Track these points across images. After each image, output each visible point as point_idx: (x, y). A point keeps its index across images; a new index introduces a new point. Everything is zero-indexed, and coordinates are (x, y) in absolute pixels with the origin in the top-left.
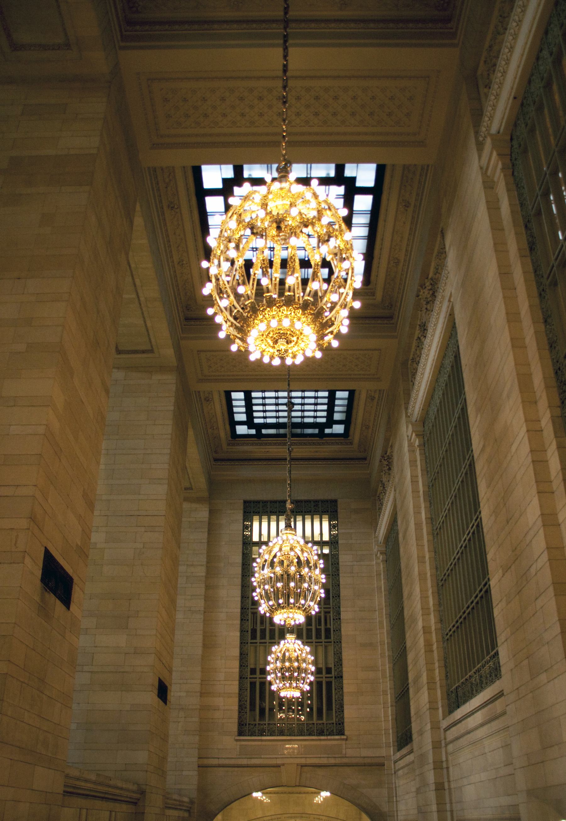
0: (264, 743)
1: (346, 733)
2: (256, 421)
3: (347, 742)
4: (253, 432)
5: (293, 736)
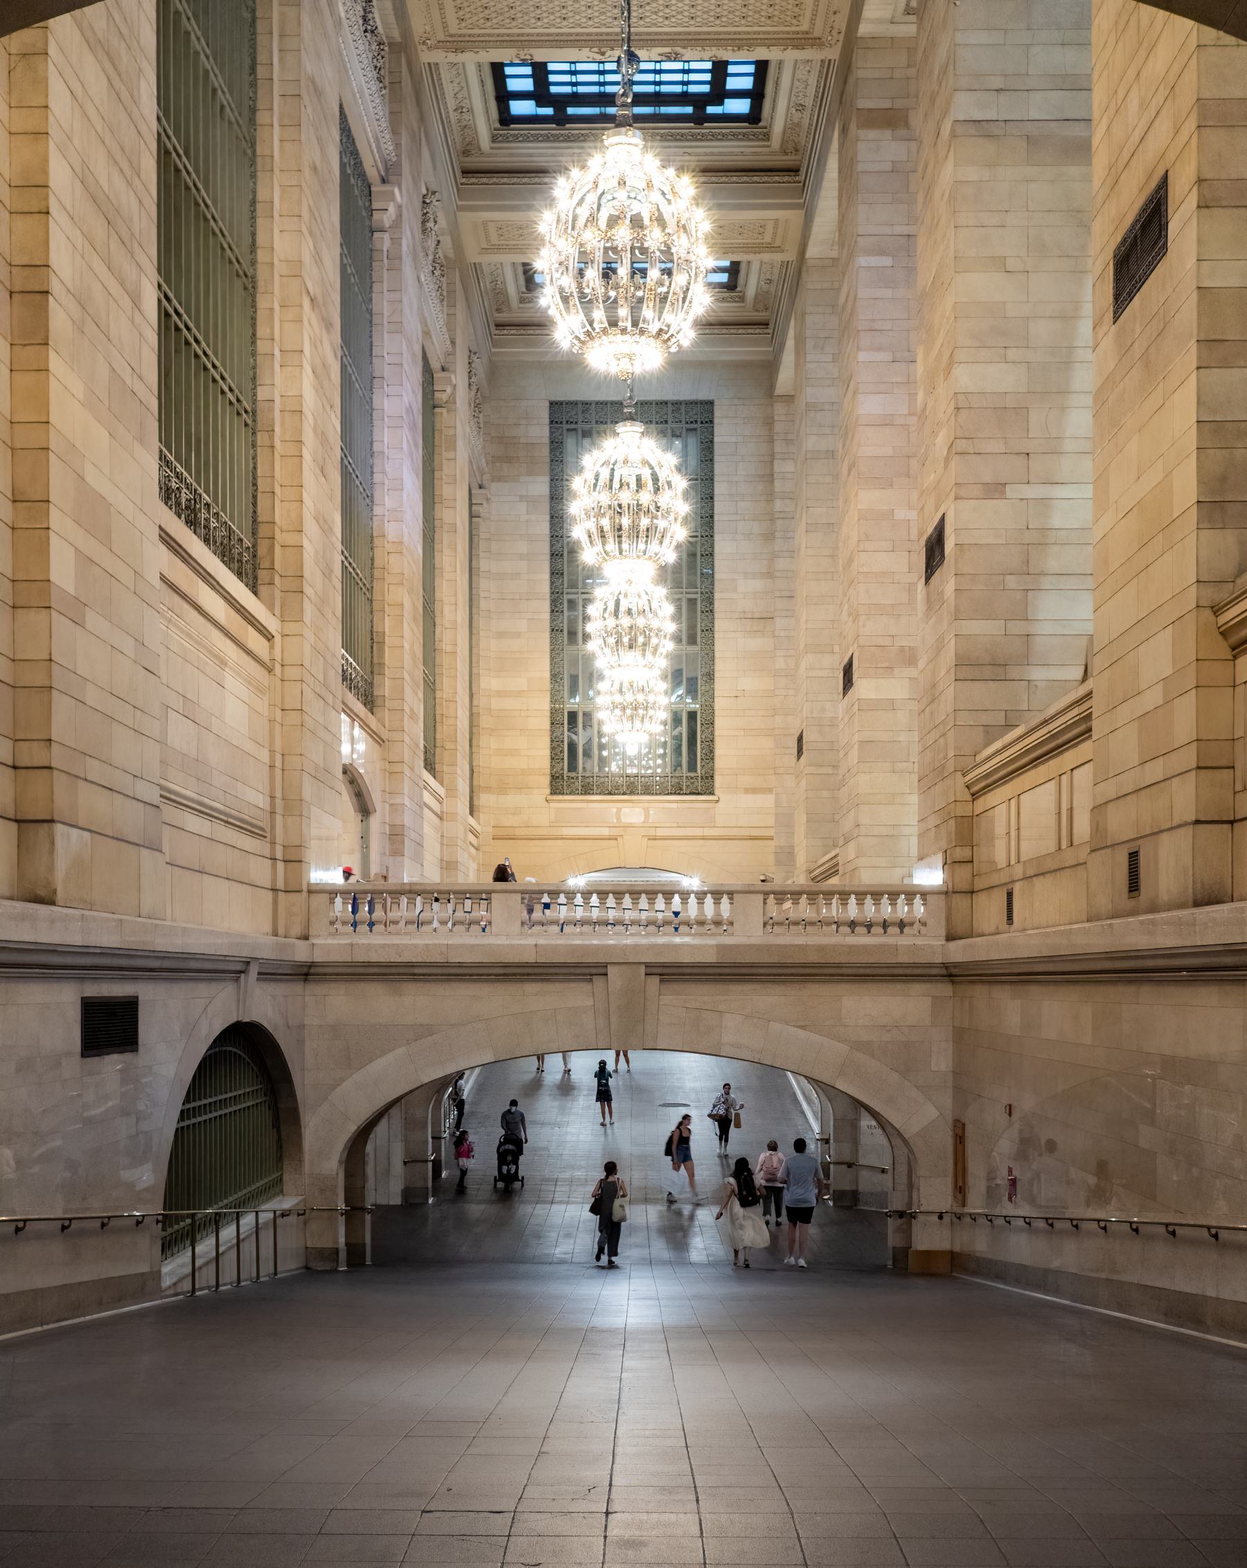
0: (591, 805)
1: (717, 792)
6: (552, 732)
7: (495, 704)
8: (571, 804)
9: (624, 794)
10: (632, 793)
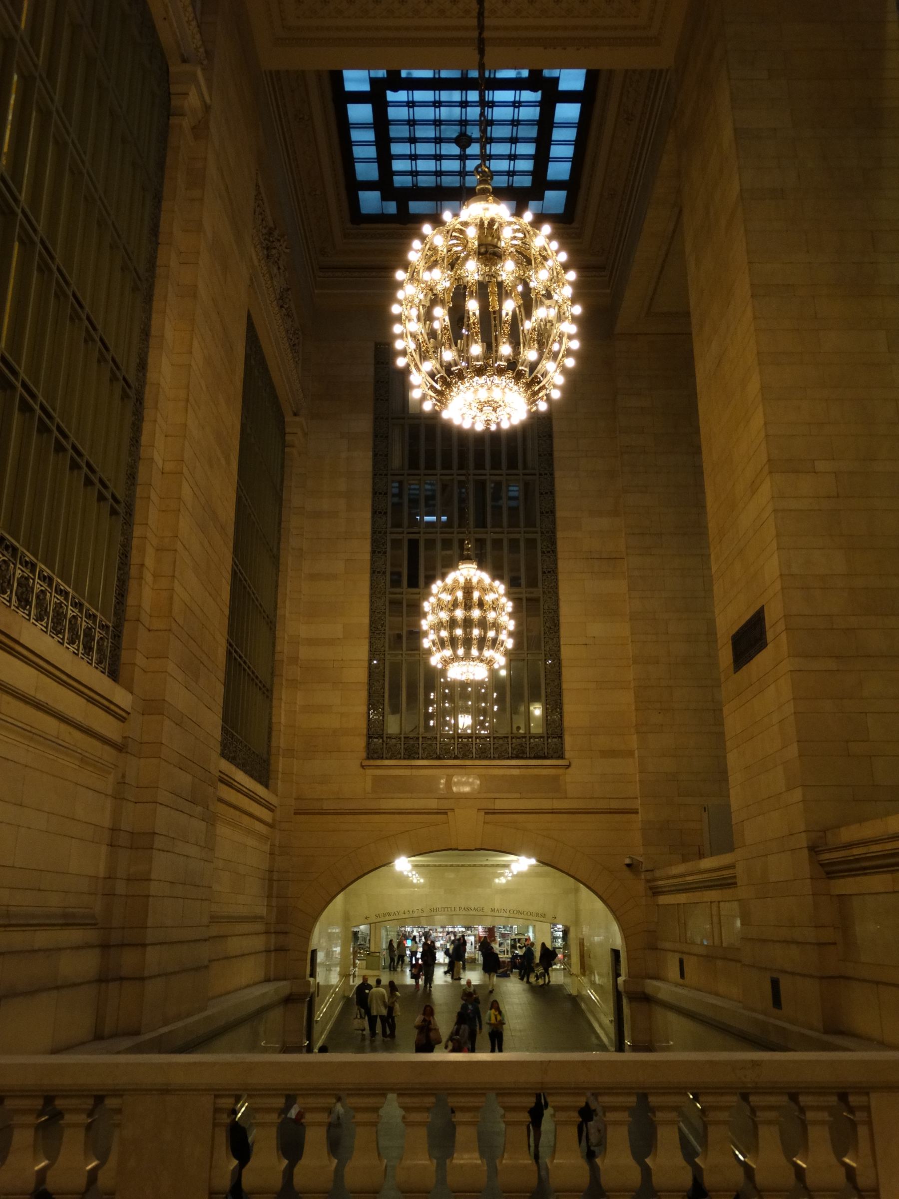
0: (415, 772)
1: (567, 755)
2: (398, 181)
3: (569, 771)
4: (391, 207)
5: (468, 759)
6: (370, 685)
7: (304, 653)
8: (394, 768)
9: (456, 758)
10: (465, 757)
